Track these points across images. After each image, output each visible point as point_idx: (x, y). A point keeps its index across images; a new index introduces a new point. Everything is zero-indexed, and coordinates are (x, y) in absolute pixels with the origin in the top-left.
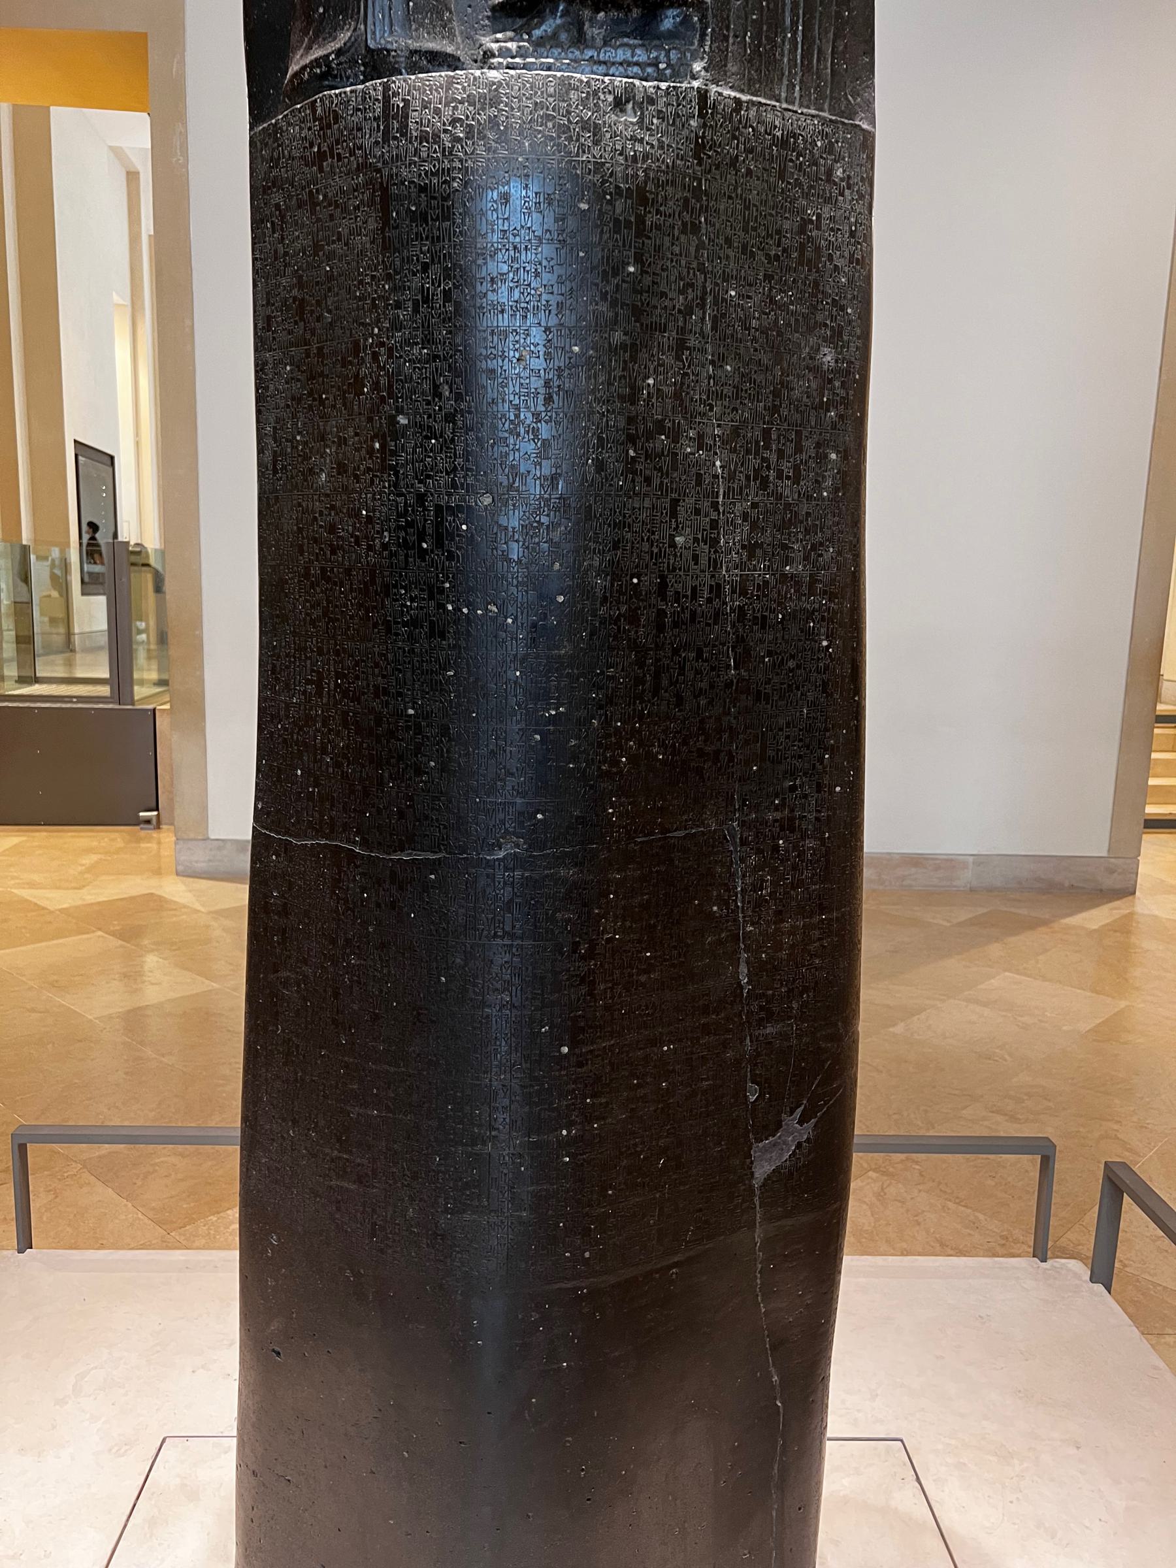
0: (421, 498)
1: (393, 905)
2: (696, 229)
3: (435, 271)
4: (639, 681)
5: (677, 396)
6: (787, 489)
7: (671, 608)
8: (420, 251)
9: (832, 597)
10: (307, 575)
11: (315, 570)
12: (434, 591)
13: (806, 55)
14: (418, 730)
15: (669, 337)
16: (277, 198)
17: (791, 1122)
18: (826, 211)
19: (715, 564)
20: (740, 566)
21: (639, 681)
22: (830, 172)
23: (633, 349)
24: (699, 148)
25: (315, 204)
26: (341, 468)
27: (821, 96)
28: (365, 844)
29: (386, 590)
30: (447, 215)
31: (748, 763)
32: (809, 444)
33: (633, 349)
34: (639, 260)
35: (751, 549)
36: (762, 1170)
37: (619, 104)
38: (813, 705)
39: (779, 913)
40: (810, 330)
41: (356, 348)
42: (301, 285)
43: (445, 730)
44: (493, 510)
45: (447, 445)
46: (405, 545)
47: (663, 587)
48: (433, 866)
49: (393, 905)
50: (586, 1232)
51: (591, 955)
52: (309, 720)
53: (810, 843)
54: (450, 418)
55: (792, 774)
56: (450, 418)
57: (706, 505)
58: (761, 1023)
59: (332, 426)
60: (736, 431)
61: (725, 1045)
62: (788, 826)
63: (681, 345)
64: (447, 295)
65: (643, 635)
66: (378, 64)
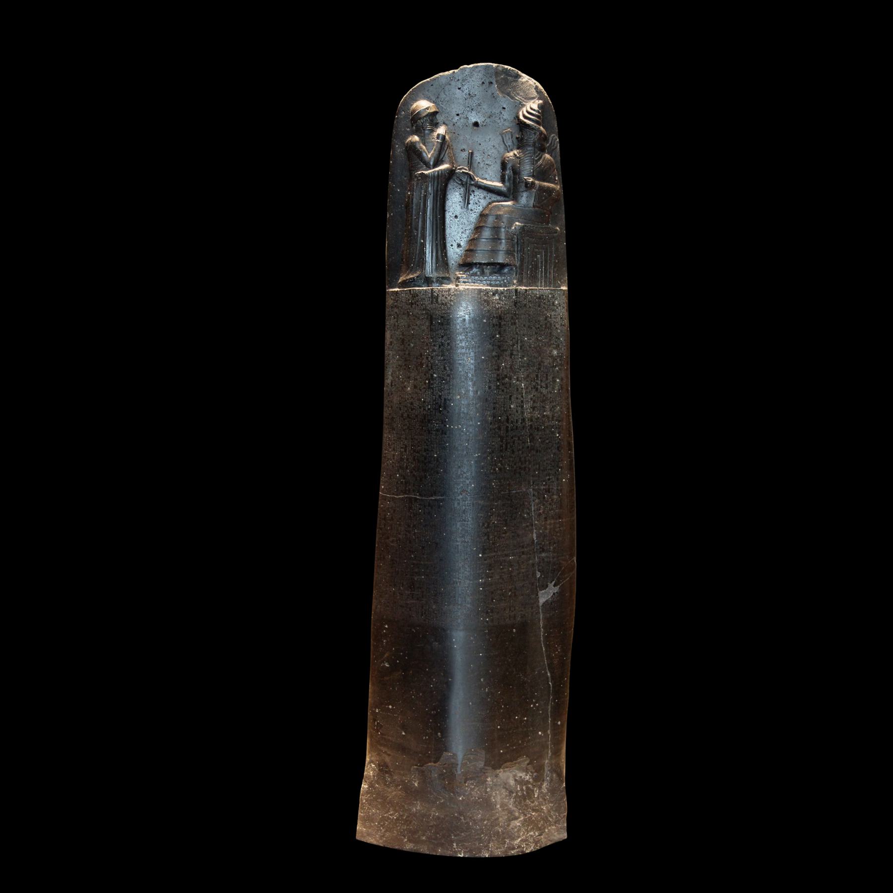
0: (440, 396)
1: (429, 513)
2: (515, 324)
3: (445, 338)
4: (502, 446)
5: (511, 368)
6: (544, 391)
7: (510, 426)
8: (441, 332)
9: (559, 421)
10: (402, 416)
11: (405, 415)
12: (443, 422)
13: (546, 273)
14: (438, 461)
15: (509, 352)
16: (396, 310)
17: (551, 585)
18: (553, 313)
19: (523, 413)
20: (531, 413)
21: (502, 446)
22: (553, 303)
23: (498, 357)
24: (515, 303)
25: (409, 315)
26: (415, 387)
27: (550, 283)
28: (420, 495)
29: (429, 421)
30: (448, 324)
31: (534, 471)
32: (550, 378)
33: (498, 357)
34: (499, 333)
35: (533, 408)
36: (542, 601)
37: (494, 294)
38: (554, 454)
39: (546, 518)
40: (549, 346)
41: (421, 355)
42: (403, 334)
43: (445, 461)
44: (460, 400)
45: (448, 383)
46: (435, 409)
47: (508, 420)
48: (442, 501)
49: (429, 513)
50: (487, 612)
51: (488, 527)
52: (402, 459)
53: (555, 497)
54: (449, 375)
55: (549, 475)
56: (449, 375)
57: (520, 396)
58: (540, 553)
59: (412, 375)
60: (528, 376)
61: (529, 559)
62: (548, 491)
63: (512, 354)
64: (448, 344)
65: (502, 433)
66: (428, 281)
